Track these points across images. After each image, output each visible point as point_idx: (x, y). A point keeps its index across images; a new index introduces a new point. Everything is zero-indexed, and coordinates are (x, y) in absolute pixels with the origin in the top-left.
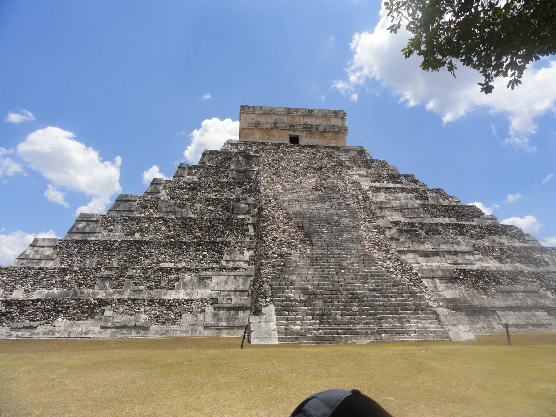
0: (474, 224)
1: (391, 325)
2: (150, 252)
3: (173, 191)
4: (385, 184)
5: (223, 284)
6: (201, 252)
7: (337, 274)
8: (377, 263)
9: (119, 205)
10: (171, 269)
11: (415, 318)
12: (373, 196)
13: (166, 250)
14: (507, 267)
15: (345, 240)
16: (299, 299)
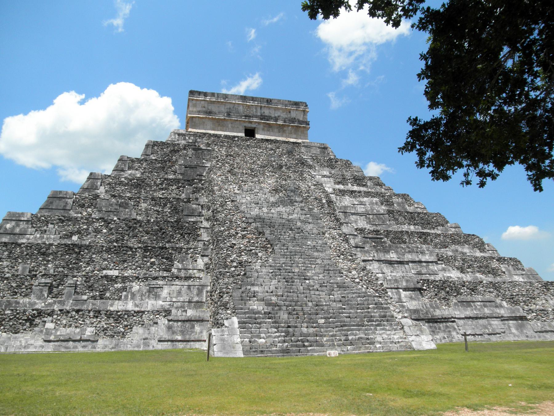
0: (439, 232)
1: (357, 337)
2: (91, 258)
3: (113, 188)
4: (350, 187)
5: (175, 295)
6: (149, 259)
7: (302, 285)
8: (342, 273)
9: (51, 203)
10: (117, 277)
12: (337, 200)
13: (109, 256)
14: (468, 277)
15: (309, 249)
16: (263, 312)
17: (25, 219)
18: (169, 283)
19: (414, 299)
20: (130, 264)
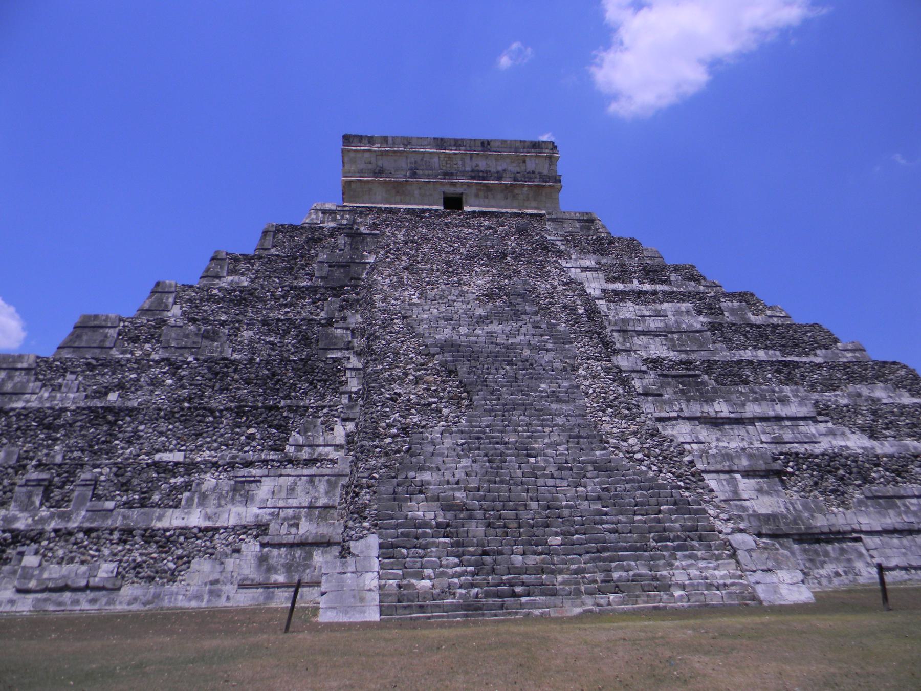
0: (819, 360)
1: (631, 573)
2: (136, 431)
3: (197, 307)
4: (636, 285)
5: (283, 495)
6: (244, 429)
7: (520, 468)
8: (608, 443)
9: (79, 337)
10: (177, 464)
11: (685, 557)
12: (609, 309)
13: (171, 427)
15: (542, 397)
16: (434, 523)
17: (25, 365)
18: (272, 472)
19: (768, 494)
20: (208, 440)
